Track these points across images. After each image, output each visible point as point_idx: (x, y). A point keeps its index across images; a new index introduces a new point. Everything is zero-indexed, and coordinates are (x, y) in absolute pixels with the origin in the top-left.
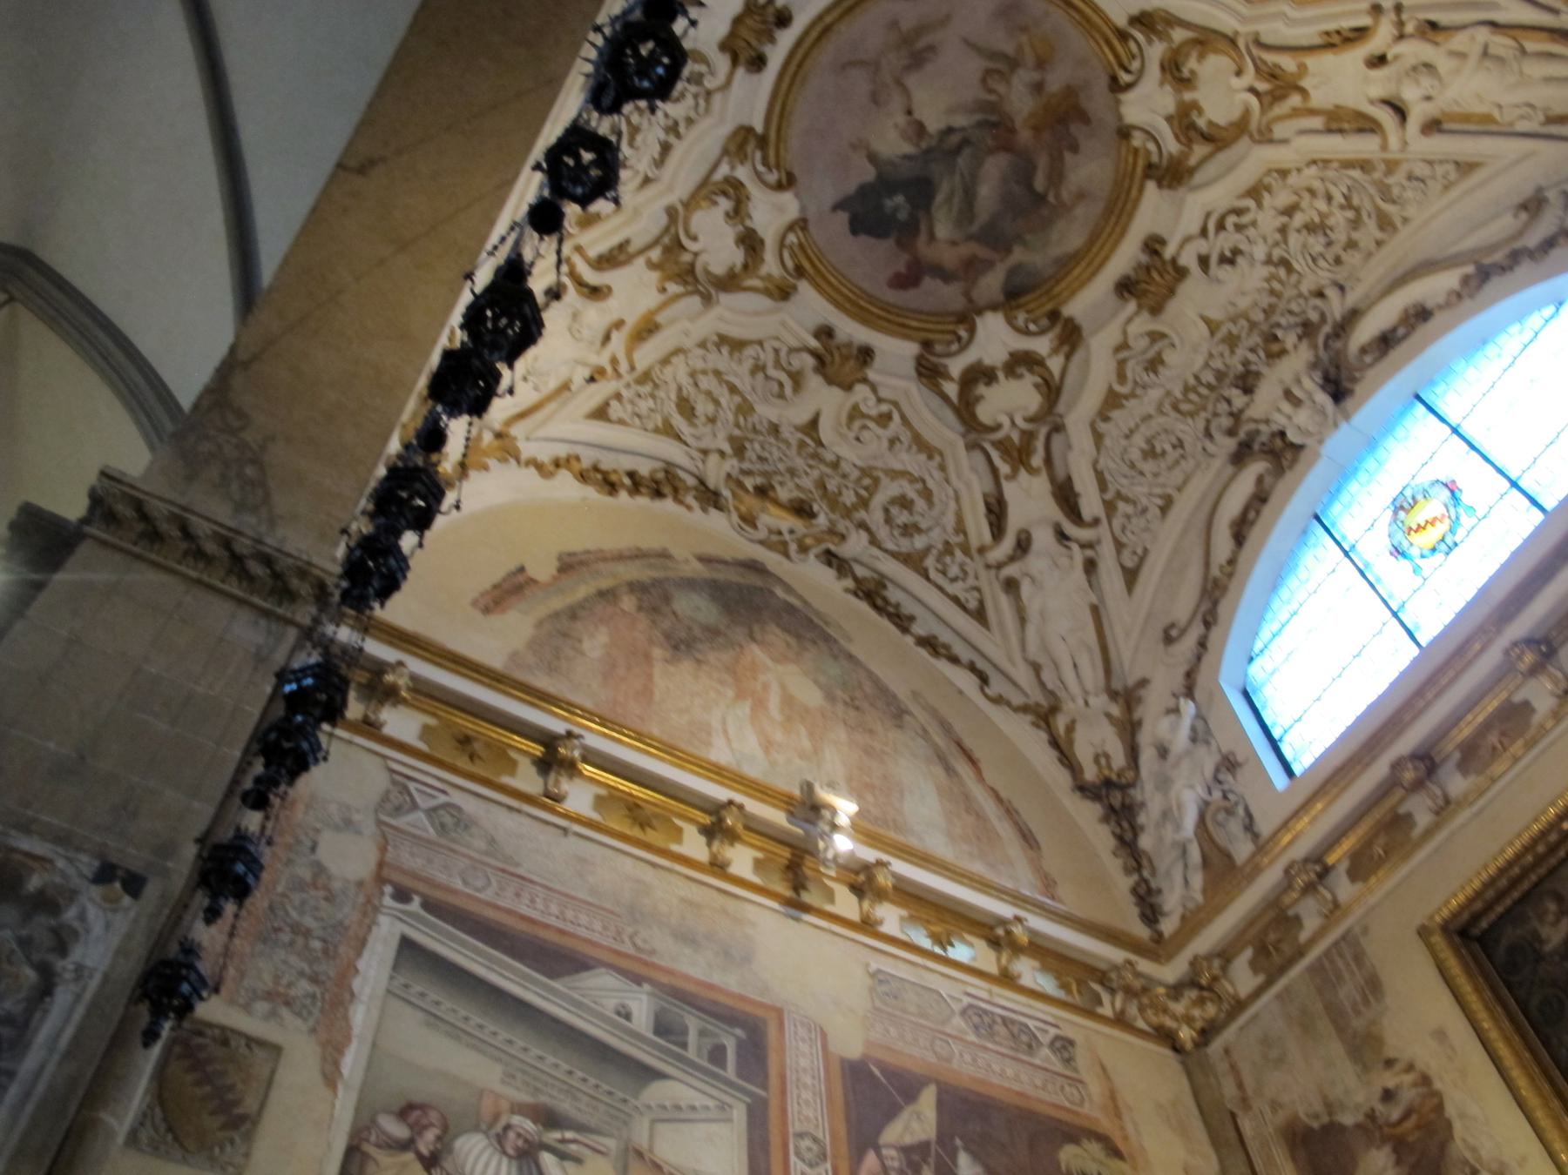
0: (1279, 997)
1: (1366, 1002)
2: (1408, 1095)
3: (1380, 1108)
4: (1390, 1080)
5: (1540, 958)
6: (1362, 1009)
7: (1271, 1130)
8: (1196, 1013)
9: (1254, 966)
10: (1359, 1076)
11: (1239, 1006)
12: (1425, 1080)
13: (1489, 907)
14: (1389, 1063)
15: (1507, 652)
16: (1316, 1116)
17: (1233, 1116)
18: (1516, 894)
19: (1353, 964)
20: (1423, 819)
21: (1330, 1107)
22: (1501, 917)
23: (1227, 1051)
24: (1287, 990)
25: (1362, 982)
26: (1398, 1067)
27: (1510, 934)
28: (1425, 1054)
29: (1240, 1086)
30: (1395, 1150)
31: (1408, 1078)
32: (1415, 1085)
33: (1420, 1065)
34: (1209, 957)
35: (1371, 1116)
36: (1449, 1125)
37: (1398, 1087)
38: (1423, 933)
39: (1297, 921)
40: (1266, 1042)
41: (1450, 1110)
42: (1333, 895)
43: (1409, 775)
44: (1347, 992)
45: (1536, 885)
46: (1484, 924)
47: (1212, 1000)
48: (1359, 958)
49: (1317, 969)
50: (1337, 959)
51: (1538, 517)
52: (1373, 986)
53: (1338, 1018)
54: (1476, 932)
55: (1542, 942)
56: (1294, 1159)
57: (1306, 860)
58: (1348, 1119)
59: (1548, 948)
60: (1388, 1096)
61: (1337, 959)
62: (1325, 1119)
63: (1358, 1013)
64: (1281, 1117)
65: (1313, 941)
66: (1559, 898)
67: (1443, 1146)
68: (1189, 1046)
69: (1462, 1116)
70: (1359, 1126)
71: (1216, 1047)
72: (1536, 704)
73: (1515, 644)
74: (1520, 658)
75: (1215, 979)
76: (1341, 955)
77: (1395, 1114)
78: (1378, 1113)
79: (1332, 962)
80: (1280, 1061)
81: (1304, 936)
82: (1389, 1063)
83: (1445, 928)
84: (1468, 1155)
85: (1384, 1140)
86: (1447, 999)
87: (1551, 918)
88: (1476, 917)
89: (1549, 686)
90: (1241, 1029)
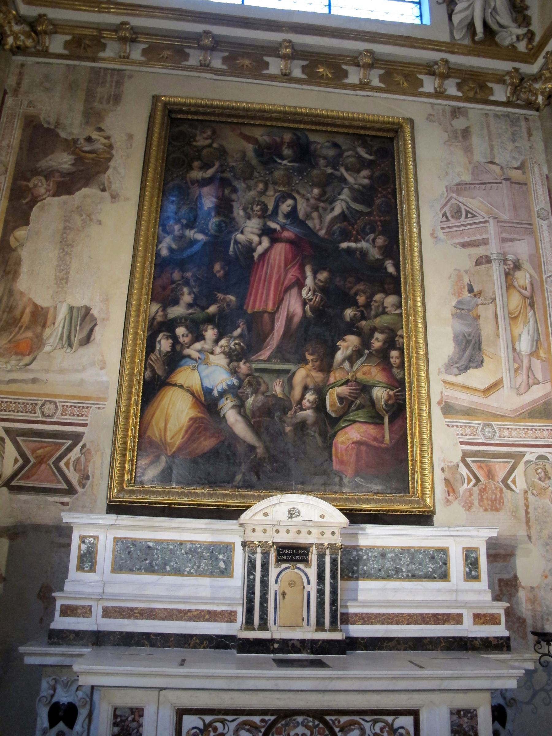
0: (68, 65)
1: (108, 101)
2: (97, 146)
3: (82, 141)
4: (95, 135)
5: (189, 144)
6: (104, 102)
7: (21, 111)
8: (22, 37)
9: (67, 44)
10: (81, 124)
11: (45, 53)
12: (111, 147)
13: (188, 113)
14: (100, 130)
15: (285, 40)
16: (49, 123)
17: (5, 93)
18: (201, 118)
19: (114, 84)
20: (193, 61)
21: (58, 124)
22: (188, 119)
23: (22, 65)
24: (74, 66)
25: (113, 93)
26: (102, 133)
27: (185, 128)
28: (118, 139)
29: (19, 84)
30: (75, 159)
31: (105, 141)
32: (104, 145)
33: (112, 140)
34: (51, 22)
35: (75, 141)
36: (107, 168)
37: (96, 140)
38: (156, 99)
39: (104, 47)
40: (46, 77)
41: (112, 164)
42: (130, 51)
43: (207, 42)
44: (101, 91)
45: (211, 121)
46: (179, 116)
47: (33, 39)
48: (119, 84)
49: (95, 71)
50: (109, 76)
51: (326, 11)
52: (117, 99)
53: (90, 96)
54: (174, 116)
55: (195, 140)
56: (24, 130)
57: (132, 28)
58: (63, 135)
59: (195, 143)
60: (89, 139)
61: (109, 76)
62: (52, 127)
63: (101, 102)
64: (31, 111)
65: (103, 59)
66: (214, 132)
67: (99, 173)
68: (7, 47)
69: (115, 169)
70: (66, 140)
71: (19, 59)
72: (271, 67)
73: (290, 42)
74: (286, 47)
75: (45, 32)
76: (112, 76)
77: (87, 148)
78: (79, 142)
79: (106, 75)
80: (47, 90)
81: (101, 55)
82: (100, 130)
83: (166, 104)
84: (106, 183)
85: (73, 153)
86: (144, 127)
87: (205, 135)
88: (181, 111)
89: (282, 66)
90: (38, 63)
